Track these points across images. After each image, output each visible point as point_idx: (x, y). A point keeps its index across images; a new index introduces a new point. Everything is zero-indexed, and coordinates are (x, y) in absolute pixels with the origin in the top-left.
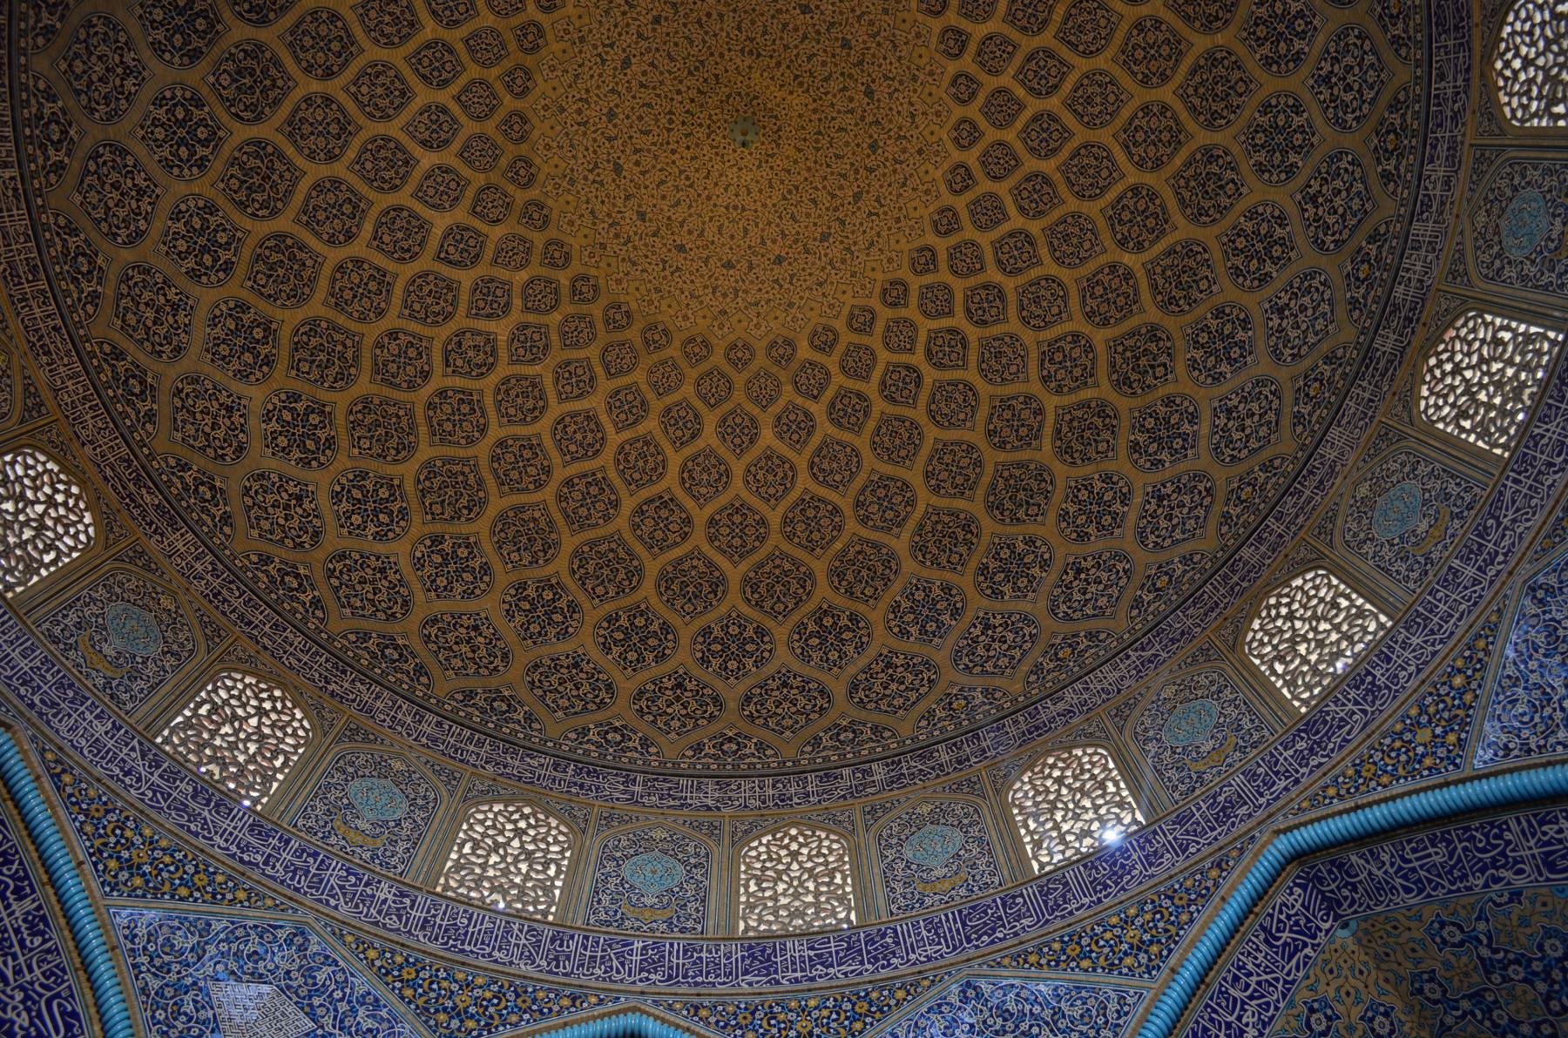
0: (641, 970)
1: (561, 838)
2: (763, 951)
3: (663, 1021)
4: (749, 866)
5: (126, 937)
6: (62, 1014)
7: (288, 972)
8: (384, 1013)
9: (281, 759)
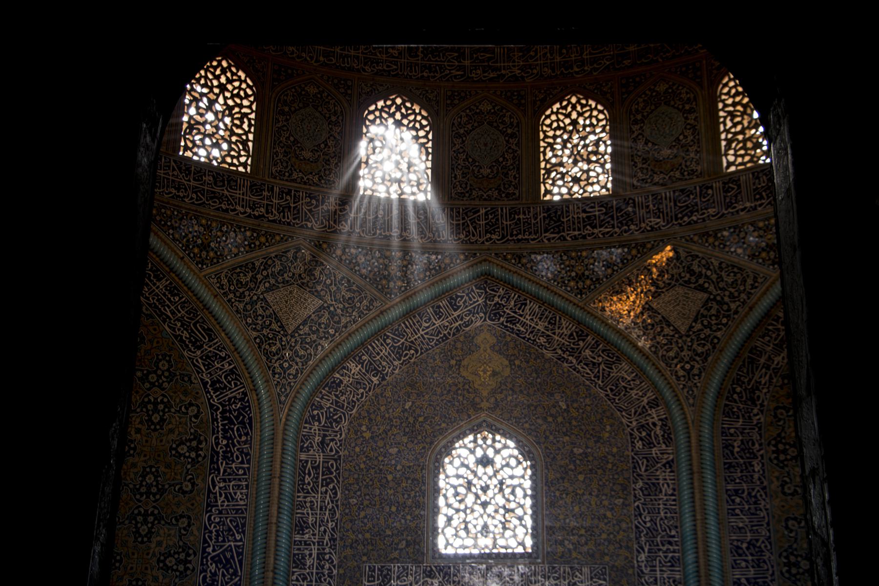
0: (487, 232)
1: (424, 122)
2: (556, 212)
3: (502, 267)
4: (546, 137)
5: (219, 288)
6: (204, 329)
7: (300, 275)
8: (354, 288)
9: (245, 120)
